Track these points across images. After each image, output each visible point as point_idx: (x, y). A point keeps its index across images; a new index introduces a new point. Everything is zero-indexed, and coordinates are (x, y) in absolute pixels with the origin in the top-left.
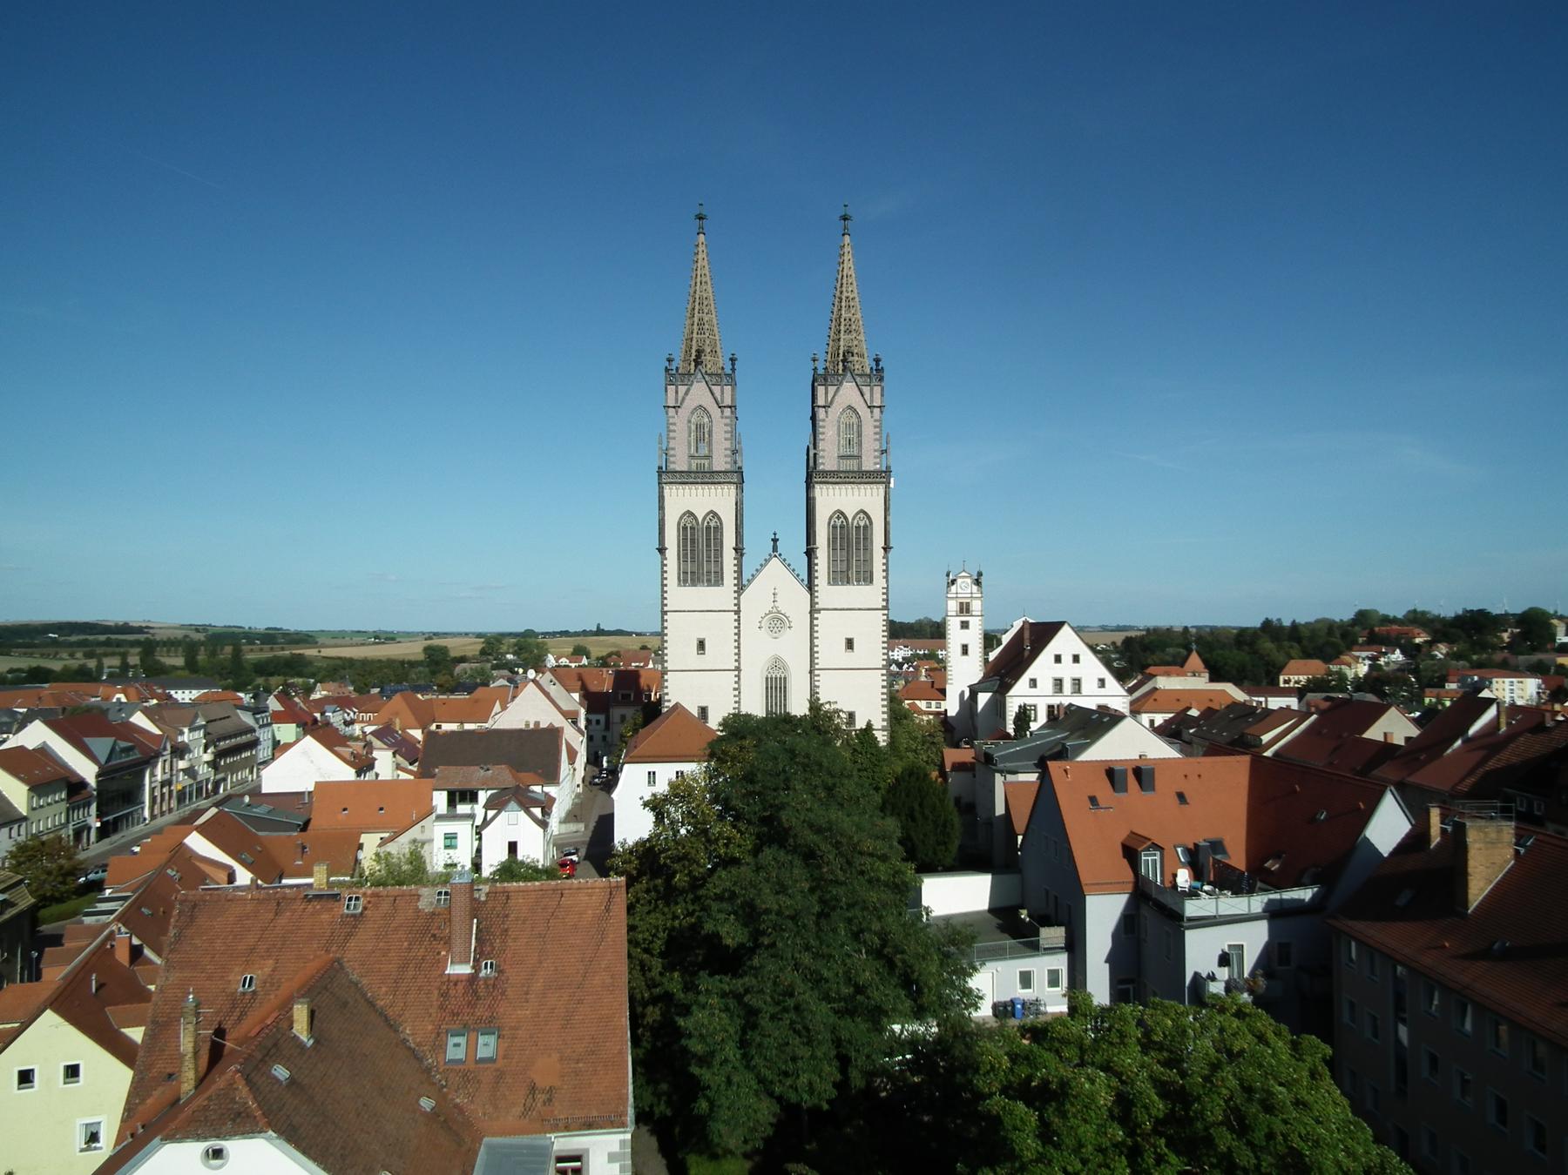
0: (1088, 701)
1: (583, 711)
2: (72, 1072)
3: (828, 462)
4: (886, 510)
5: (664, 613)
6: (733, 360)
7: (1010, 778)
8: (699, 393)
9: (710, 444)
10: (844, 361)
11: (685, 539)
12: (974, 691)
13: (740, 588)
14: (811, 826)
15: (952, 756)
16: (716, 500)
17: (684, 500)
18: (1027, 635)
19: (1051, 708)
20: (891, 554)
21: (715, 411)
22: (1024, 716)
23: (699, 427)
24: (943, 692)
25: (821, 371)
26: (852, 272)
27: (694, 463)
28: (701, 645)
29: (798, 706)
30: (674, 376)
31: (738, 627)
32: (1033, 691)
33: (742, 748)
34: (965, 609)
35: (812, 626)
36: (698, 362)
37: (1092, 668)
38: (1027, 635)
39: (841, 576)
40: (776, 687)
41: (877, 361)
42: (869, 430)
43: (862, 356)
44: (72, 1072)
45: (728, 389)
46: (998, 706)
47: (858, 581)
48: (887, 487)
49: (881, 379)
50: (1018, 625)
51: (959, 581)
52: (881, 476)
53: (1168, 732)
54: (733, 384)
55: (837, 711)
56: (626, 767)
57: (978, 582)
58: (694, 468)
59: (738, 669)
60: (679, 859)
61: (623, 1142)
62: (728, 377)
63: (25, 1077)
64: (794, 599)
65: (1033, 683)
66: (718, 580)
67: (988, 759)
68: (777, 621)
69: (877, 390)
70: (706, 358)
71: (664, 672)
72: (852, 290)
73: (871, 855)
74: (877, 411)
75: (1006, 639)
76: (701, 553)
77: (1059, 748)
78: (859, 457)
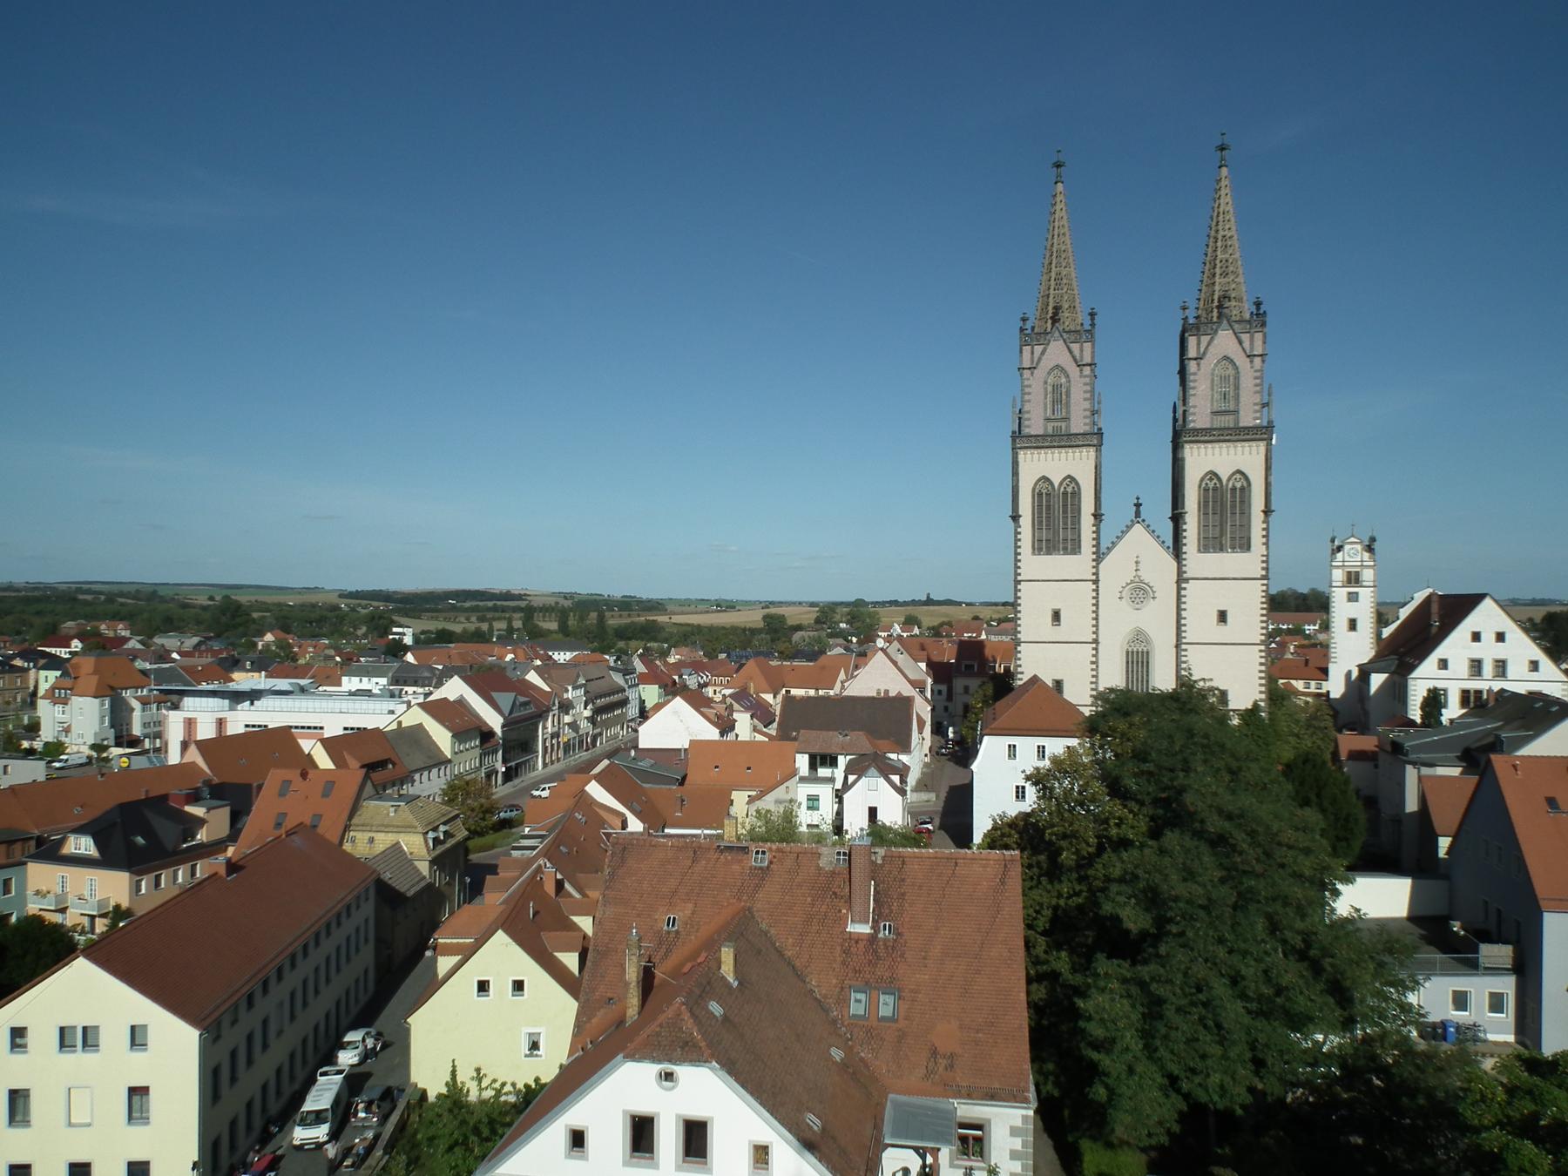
0: (1519, 682)
1: (930, 681)
2: (519, 986)
3: (1200, 417)
4: (1268, 468)
5: (1017, 582)
6: (1092, 315)
7: (1425, 771)
8: (1056, 352)
9: (1068, 404)
10: (1220, 307)
11: (1040, 506)
12: (1365, 672)
13: (1099, 557)
14: (1220, 811)
15: (1349, 742)
16: (1075, 465)
17: (1039, 465)
18: (1435, 608)
20: (1272, 517)
21: (1073, 370)
22: (1434, 701)
23: (1056, 388)
24: (1324, 672)
25: (1191, 321)
26: (1229, 208)
27: (1050, 426)
28: (1056, 616)
29: (1163, 680)
30: (1030, 336)
31: (1096, 598)
32: (1443, 673)
33: (1131, 725)
34: (1353, 579)
35: (1179, 596)
36: (1055, 320)
37: (1522, 649)
38: (1435, 608)
39: (1212, 543)
40: (1138, 661)
41: (1258, 304)
42: (1248, 382)
43: (1240, 300)
44: (519, 986)
45: (1087, 346)
46: (1397, 691)
47: (1233, 548)
48: (1269, 445)
49: (1263, 324)
50: (1420, 597)
51: (1347, 547)
52: (1262, 433)
54: (1092, 340)
55: (1212, 689)
56: (986, 738)
57: (1370, 549)
58: (1050, 431)
59: (1096, 641)
60: (1065, 836)
61: (1025, 1118)
62: (1087, 334)
63: (483, 987)
64: (1159, 568)
65: (1443, 664)
66: (1075, 548)
67: (1397, 748)
68: (1140, 592)
69: (1258, 337)
70: (1064, 314)
71: (1018, 643)
72: (1229, 228)
73: (1290, 847)
74: (1257, 360)
75: (1404, 613)
76: (1057, 518)
77: (1491, 739)
78: (1236, 412)
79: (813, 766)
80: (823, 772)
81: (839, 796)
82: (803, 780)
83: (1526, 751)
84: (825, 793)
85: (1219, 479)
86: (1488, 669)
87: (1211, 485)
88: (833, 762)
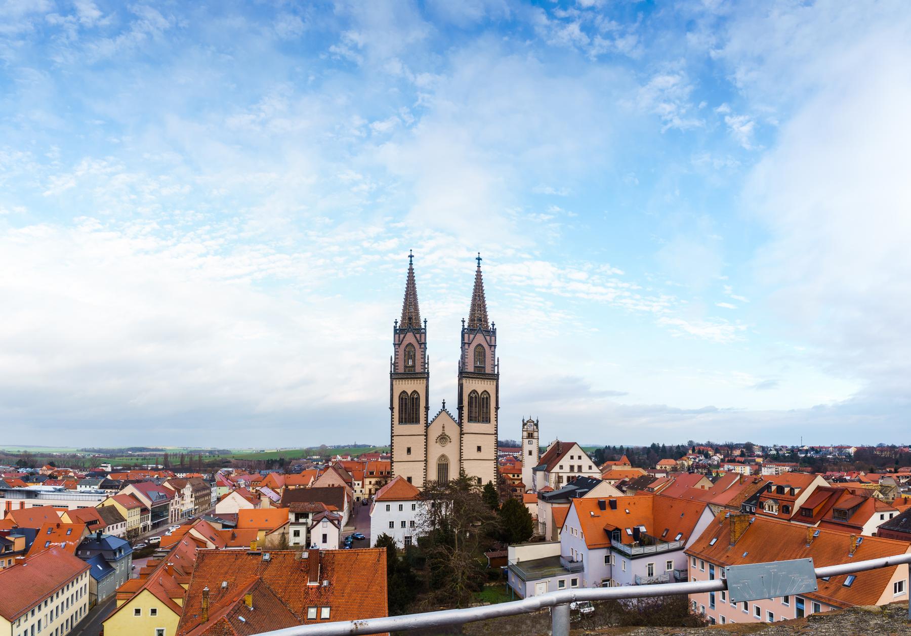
19: (568, 477)
37: (586, 462)
40: (443, 468)
53: (619, 487)
59: (426, 460)
65: (561, 467)
79: (297, 519)
80: (302, 520)
81: (308, 531)
82: (292, 524)
83: (587, 496)
84: (303, 530)
86: (576, 469)
87: (474, 396)
88: (307, 516)
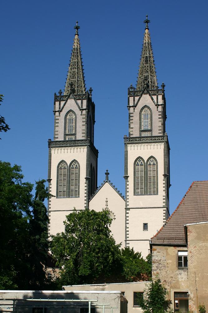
58: (67, 139)
85: (143, 160)
